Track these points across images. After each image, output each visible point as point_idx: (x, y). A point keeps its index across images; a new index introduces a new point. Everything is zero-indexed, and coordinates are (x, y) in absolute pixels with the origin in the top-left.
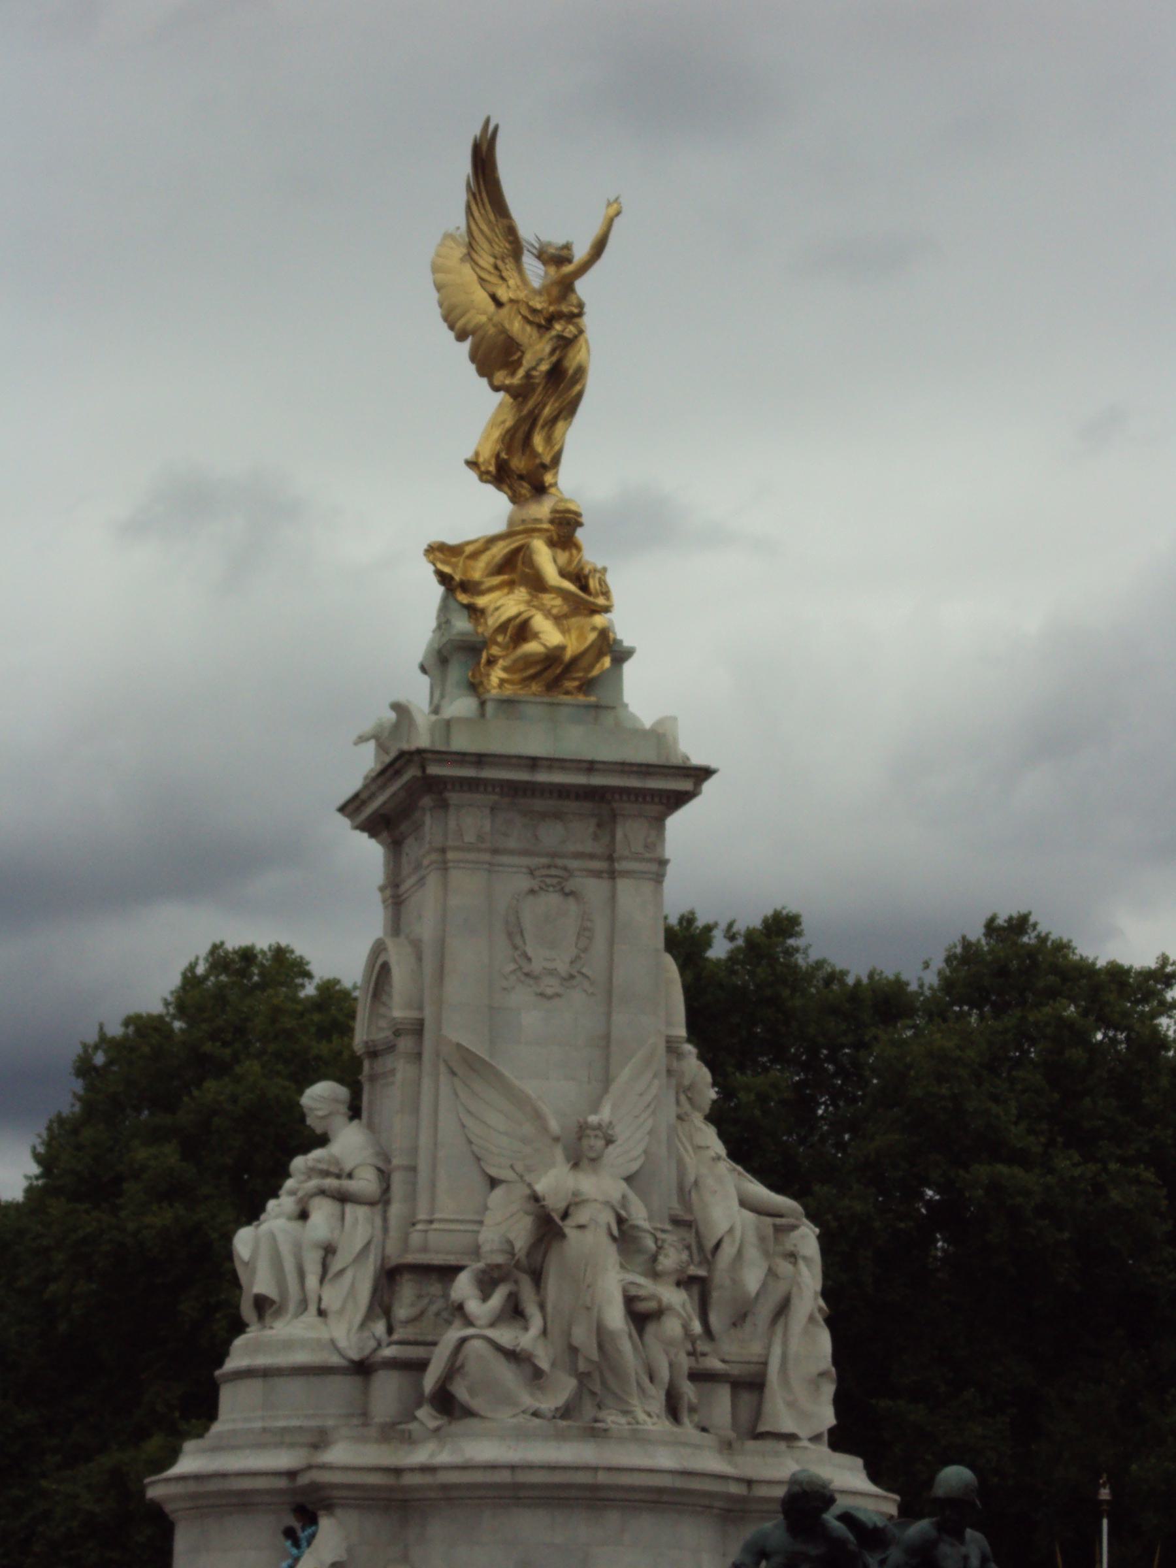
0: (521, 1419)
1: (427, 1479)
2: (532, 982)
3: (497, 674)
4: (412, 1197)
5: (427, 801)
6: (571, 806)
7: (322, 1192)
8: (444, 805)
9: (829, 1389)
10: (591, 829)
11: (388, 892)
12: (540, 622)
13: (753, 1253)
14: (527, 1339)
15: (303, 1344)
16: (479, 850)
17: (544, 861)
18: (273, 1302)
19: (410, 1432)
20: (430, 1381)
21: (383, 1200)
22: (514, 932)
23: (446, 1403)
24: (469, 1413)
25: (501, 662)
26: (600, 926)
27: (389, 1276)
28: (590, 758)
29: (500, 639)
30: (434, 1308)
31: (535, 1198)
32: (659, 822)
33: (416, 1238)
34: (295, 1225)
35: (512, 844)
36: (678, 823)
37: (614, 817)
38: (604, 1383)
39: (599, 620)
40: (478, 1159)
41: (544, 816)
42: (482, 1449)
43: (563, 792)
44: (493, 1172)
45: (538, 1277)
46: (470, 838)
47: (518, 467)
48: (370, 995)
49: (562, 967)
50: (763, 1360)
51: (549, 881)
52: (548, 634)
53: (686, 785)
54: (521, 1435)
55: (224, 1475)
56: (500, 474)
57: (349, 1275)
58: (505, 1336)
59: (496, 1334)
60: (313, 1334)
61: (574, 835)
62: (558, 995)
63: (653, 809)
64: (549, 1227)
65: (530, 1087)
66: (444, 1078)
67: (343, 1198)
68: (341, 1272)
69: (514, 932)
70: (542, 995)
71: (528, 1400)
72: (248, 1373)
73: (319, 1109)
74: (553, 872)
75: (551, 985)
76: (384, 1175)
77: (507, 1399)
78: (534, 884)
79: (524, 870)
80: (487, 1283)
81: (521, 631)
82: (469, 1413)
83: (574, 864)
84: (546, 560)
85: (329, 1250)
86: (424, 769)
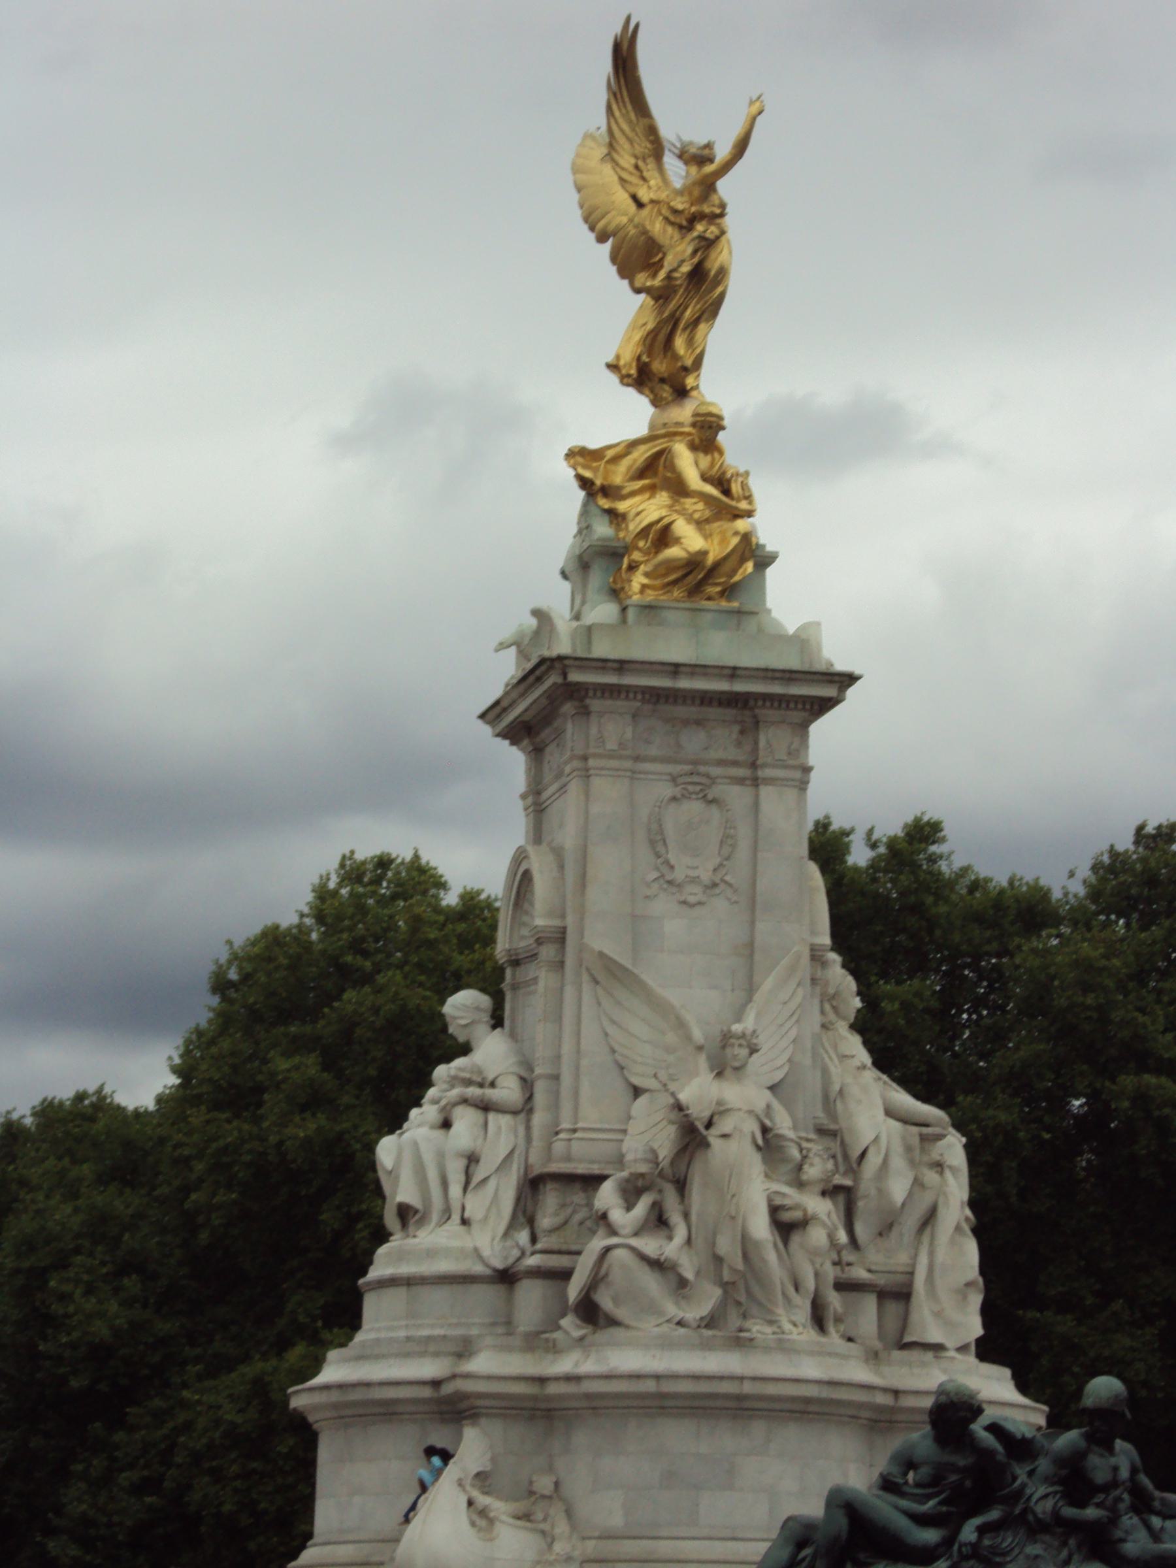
0: (665, 1328)
1: (570, 1388)
2: (674, 890)
3: (638, 580)
4: (555, 1105)
5: (568, 708)
6: (714, 712)
7: (465, 1101)
8: (585, 712)
9: (976, 1300)
10: (734, 736)
11: (530, 800)
12: (682, 528)
13: (898, 1162)
14: (671, 1248)
15: (447, 1252)
16: (620, 757)
18: (416, 1211)
19: (554, 1341)
20: (574, 1290)
21: (526, 1109)
22: (657, 841)
23: (590, 1312)
24: (613, 1322)
25: (642, 567)
26: (744, 832)
27: (533, 1184)
28: (732, 664)
29: (641, 544)
30: (578, 1217)
31: (679, 1107)
32: (803, 728)
33: (559, 1147)
34: (439, 1133)
35: (653, 751)
36: (822, 729)
38: (749, 1293)
39: (741, 525)
40: (622, 1068)
41: (686, 723)
42: (626, 1358)
43: (705, 699)
44: (636, 1081)
45: (681, 1185)
46: (611, 745)
47: (658, 371)
48: (511, 907)
49: (706, 876)
50: (909, 1269)
51: (691, 788)
52: (691, 539)
53: (829, 692)
54: (666, 1344)
55: (368, 1385)
56: (641, 377)
58: (650, 1245)
59: (640, 1243)
60: (456, 1243)
61: (717, 742)
62: (700, 903)
63: (797, 716)
64: (693, 1137)
65: (673, 996)
66: (587, 987)
67: (486, 1107)
68: (485, 1180)
69: (657, 841)
70: (684, 902)
71: (672, 1309)
72: (392, 1282)
73: (462, 1018)
74: (695, 779)
75: (694, 893)
76: (527, 1084)
77: (653, 1309)
78: (677, 791)
79: (668, 777)
80: (631, 1192)
81: (663, 536)
82: (613, 1322)
83: (715, 771)
84: (688, 464)
85: (472, 1159)
86: (565, 675)
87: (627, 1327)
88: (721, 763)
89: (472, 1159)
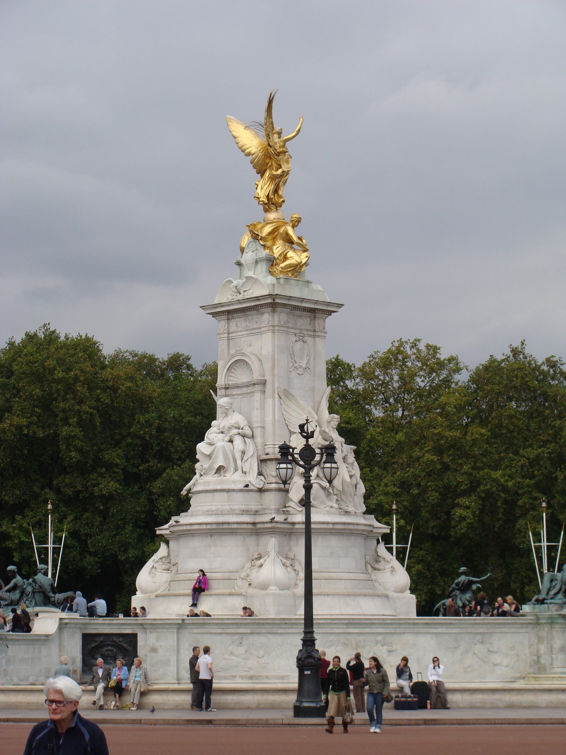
5: (269, 309)
6: (305, 313)
7: (239, 434)
17: (298, 331)
22: (292, 354)
34: (230, 444)
36: (330, 320)
37: (315, 317)
44: (292, 430)
52: (294, 257)
54: (329, 513)
55: (228, 523)
57: (249, 460)
77: (323, 503)
83: (306, 332)
85: (243, 453)
87: (316, 507)
88: (307, 330)
89: (243, 453)
